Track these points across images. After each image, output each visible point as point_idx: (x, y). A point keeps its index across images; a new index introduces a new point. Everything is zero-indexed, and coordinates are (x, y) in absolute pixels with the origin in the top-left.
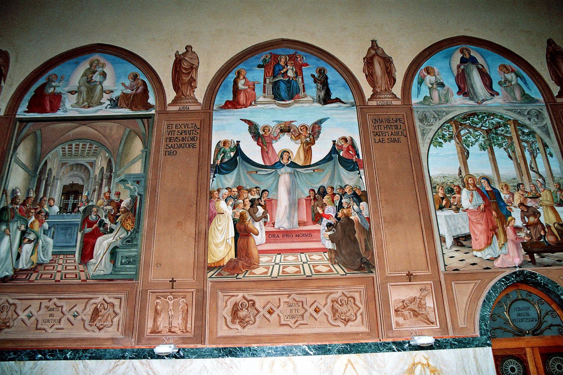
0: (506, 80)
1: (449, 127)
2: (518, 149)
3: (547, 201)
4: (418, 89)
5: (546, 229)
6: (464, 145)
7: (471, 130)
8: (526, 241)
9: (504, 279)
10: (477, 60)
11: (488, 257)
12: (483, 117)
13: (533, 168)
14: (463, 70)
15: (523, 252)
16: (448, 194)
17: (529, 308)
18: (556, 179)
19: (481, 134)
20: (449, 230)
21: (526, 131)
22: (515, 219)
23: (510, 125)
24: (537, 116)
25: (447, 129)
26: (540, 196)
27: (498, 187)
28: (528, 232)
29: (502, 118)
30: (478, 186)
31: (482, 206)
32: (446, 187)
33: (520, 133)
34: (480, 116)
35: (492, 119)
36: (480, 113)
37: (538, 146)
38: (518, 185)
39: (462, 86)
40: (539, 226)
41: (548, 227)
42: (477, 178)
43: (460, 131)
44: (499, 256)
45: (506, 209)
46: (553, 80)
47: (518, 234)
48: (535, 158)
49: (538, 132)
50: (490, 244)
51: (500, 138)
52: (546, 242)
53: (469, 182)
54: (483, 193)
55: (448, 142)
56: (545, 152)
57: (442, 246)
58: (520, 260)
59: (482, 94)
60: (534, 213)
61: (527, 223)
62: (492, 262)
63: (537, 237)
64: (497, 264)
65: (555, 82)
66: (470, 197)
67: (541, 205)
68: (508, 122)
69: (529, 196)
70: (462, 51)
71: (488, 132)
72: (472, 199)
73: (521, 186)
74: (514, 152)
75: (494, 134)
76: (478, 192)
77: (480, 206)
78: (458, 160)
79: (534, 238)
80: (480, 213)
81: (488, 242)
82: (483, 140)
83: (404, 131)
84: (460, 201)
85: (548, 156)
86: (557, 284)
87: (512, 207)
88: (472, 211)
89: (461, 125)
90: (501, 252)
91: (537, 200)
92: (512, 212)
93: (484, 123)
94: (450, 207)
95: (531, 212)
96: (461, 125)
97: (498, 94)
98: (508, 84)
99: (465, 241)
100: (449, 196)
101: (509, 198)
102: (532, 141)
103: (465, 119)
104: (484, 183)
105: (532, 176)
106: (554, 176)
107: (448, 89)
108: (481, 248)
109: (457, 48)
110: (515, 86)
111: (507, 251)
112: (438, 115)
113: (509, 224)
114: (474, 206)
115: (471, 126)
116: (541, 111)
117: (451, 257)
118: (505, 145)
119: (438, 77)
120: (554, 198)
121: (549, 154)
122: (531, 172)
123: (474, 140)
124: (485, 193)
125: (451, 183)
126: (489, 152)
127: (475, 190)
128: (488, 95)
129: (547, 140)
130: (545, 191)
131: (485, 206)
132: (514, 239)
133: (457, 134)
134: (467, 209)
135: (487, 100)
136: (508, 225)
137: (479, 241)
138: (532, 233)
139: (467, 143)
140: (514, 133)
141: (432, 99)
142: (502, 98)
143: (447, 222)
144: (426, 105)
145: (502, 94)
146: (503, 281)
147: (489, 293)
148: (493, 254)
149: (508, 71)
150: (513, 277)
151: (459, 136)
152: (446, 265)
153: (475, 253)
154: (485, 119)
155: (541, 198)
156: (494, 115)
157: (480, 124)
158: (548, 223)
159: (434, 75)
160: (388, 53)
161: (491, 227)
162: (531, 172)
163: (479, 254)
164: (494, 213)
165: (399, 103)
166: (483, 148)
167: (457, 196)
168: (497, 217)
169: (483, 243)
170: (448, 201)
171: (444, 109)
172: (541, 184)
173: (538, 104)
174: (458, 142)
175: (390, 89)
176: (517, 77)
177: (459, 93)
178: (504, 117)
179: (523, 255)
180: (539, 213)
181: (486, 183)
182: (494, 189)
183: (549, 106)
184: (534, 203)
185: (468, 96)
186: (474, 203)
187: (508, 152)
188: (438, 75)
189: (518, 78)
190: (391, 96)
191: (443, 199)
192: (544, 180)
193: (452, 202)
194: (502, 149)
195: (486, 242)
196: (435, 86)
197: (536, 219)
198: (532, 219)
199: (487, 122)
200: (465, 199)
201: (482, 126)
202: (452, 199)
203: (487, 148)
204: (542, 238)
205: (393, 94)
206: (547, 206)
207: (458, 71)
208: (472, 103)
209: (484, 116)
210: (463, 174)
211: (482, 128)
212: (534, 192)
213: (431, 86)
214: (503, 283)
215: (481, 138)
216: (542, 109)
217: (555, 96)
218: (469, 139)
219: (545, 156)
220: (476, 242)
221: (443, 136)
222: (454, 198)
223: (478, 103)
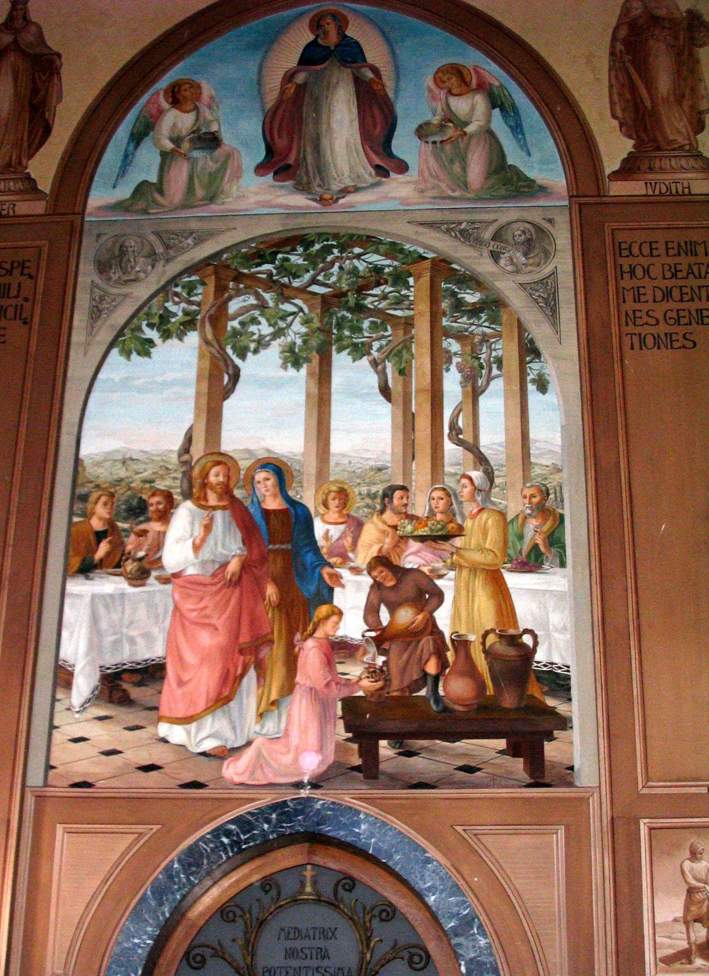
0: (450, 118)
1: (190, 288)
2: (421, 364)
3: (482, 550)
4: (126, 156)
5: (450, 655)
6: (229, 351)
7: (267, 296)
8: (361, 693)
9: (233, 827)
10: (361, 51)
11: (208, 745)
12: (327, 250)
13: (460, 431)
14: (301, 88)
15: (341, 732)
16: (125, 519)
17: (327, 934)
18: (536, 471)
19: (301, 310)
20: (95, 645)
21: (471, 297)
22: (340, 613)
23: (418, 278)
24: (528, 246)
25: (185, 294)
26: (460, 531)
27: (308, 498)
28: (380, 660)
29: (394, 250)
30: (238, 493)
31: (234, 566)
32: (122, 494)
33: (445, 305)
34: (317, 247)
35: (358, 257)
36: (320, 235)
37: (500, 353)
38: (388, 494)
39: (280, 143)
40: (426, 643)
41: (461, 644)
42: (244, 464)
43: (230, 298)
44: (249, 743)
45: (321, 576)
46: (614, 116)
47: (340, 668)
48: (474, 393)
49: (517, 300)
50: (228, 700)
51: (366, 324)
52: (438, 699)
53: (212, 479)
54: (251, 517)
55: (174, 341)
56: (523, 374)
57: (54, 700)
58: (322, 762)
59: (346, 171)
60: (421, 592)
61: (384, 629)
62: (215, 763)
63: (406, 683)
64: (234, 770)
65: (621, 126)
66: (199, 531)
67: (452, 567)
68: (413, 269)
69: (420, 532)
70: (316, 24)
71: (327, 303)
72: (203, 540)
73: (398, 494)
74: (403, 372)
75: (349, 309)
76: (234, 515)
77: (224, 565)
78: (192, 404)
79: (395, 683)
80: (220, 590)
81: (220, 694)
82: (304, 330)
83: (27, 306)
84: (159, 545)
85: (531, 387)
86: (425, 851)
87: (345, 573)
88: (194, 583)
89: (239, 277)
90: (258, 728)
91: (446, 546)
92: (337, 591)
93: (323, 270)
94: (118, 566)
95: (408, 588)
96: (239, 277)
97: (402, 167)
98: (450, 132)
99: (140, 684)
100: (126, 526)
101: (340, 538)
102: (484, 335)
103: (259, 257)
104: (265, 482)
105: (447, 460)
106: (533, 460)
107: (228, 156)
108: (189, 714)
109: (301, 14)
110: (474, 141)
111: (283, 726)
112: (167, 247)
113: (314, 630)
114: (204, 563)
115: (270, 283)
116: (547, 226)
117: (76, 740)
118: (378, 350)
119: (207, 114)
120: (511, 538)
121: (533, 381)
122: (449, 447)
123: (271, 330)
124: (258, 518)
125: (145, 481)
126: (310, 374)
127: (224, 508)
128: (367, 173)
129: (540, 331)
130: (484, 515)
131: (245, 566)
132: (320, 685)
133: (212, 312)
134: (176, 575)
135: (357, 190)
136: (311, 635)
137: (190, 686)
138: (393, 665)
139: (243, 341)
140: (424, 307)
141: (161, 192)
142: (416, 183)
143: (95, 619)
144: (136, 212)
145: (421, 173)
146: (228, 834)
147: (169, 872)
148: (229, 734)
149: (464, 88)
150: (268, 821)
151: (218, 318)
152: (53, 767)
153: (164, 729)
154: (329, 258)
155: (458, 542)
156: (369, 241)
157: (307, 277)
158: (463, 631)
159: (196, 108)
160: (53, 41)
161: (245, 638)
162: (449, 447)
163: (176, 734)
164: (271, 591)
165: (39, 207)
166: (293, 358)
167: (155, 526)
168: (279, 605)
169: (203, 690)
170: (118, 545)
171: (194, 225)
172: (476, 490)
173: (541, 203)
174: (210, 336)
175: (24, 162)
176: (494, 107)
177: (261, 169)
178: (402, 251)
179: (338, 746)
180: (439, 596)
181: (269, 483)
182: (292, 503)
183: (576, 208)
184: (429, 556)
185: (292, 177)
186: (206, 553)
187: (383, 375)
188: (210, 107)
189: (497, 112)
190: (20, 185)
191: (100, 536)
192: (490, 476)
193: (129, 547)
194: (365, 361)
195: (213, 695)
196: (186, 146)
197: (420, 617)
198: (406, 616)
199: (336, 269)
200: (178, 541)
201: (314, 281)
202: (133, 537)
203: (308, 360)
204: (425, 684)
205: (28, 178)
206: (474, 569)
207: (282, 92)
208: (300, 200)
209: (333, 246)
210: (197, 450)
211: (315, 288)
212: (439, 517)
213: (169, 145)
214: (225, 840)
215: (298, 327)
216: (550, 221)
217: (607, 171)
218: (253, 328)
219: (516, 387)
220: (179, 692)
221: (165, 317)
222: (144, 533)
223: (321, 200)
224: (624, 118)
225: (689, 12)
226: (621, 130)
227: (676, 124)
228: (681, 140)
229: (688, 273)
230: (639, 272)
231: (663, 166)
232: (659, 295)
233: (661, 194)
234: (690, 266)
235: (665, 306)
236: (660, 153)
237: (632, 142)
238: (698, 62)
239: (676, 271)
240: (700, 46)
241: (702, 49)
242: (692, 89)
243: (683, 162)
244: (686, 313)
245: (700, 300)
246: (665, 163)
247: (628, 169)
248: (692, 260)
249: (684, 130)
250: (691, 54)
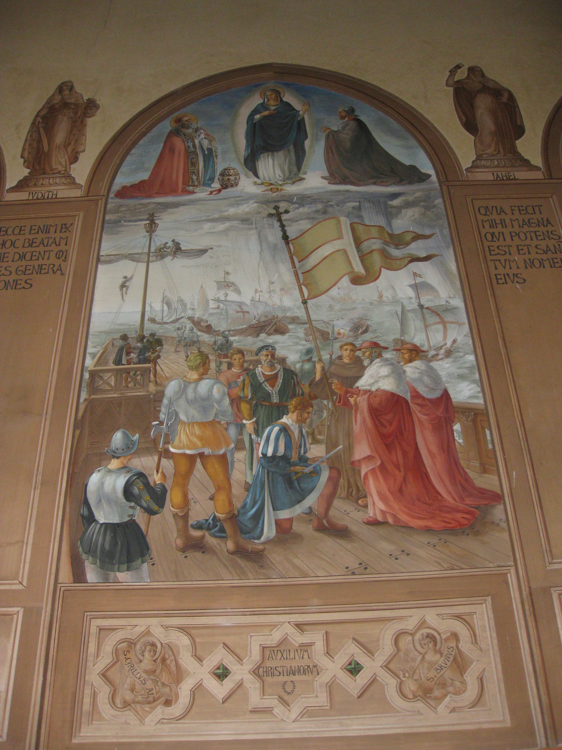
46: (22, 157)
217: (8, 186)
224: (28, 158)
225: (89, 100)
226: (24, 164)
227: (60, 160)
228: (60, 168)
229: (40, 243)
230: (8, 244)
231: (44, 183)
232: (17, 257)
233: (37, 199)
234: (42, 240)
235: (20, 263)
236: (44, 176)
237: (29, 170)
238: (85, 126)
239: (32, 243)
240: (90, 117)
241: (90, 119)
242: (76, 140)
243: (58, 180)
244: (31, 268)
245: (43, 259)
246: (46, 182)
247: (21, 185)
248: (44, 236)
249: (64, 164)
250: (82, 121)
